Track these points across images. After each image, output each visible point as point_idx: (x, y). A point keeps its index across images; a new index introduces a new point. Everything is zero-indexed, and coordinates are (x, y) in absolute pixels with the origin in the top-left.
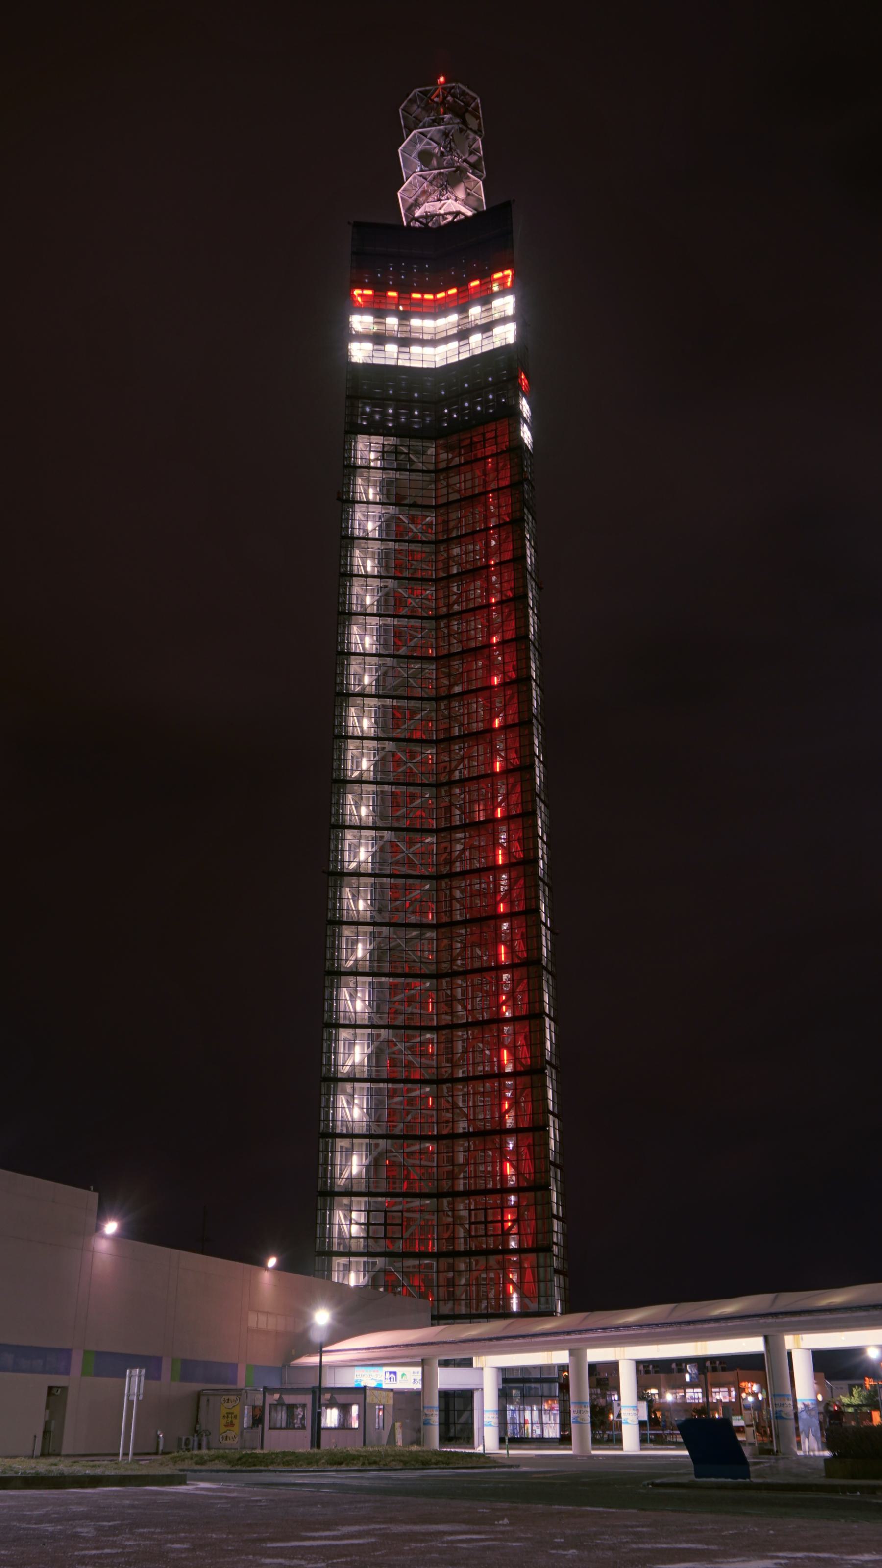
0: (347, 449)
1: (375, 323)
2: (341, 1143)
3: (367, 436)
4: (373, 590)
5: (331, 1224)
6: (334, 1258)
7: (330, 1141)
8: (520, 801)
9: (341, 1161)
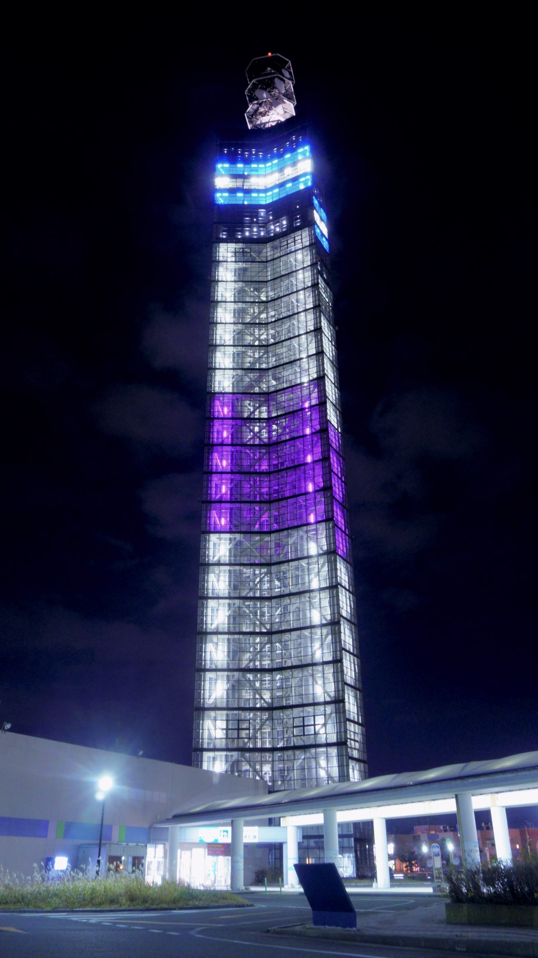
2: (209, 675)
4: (230, 331)
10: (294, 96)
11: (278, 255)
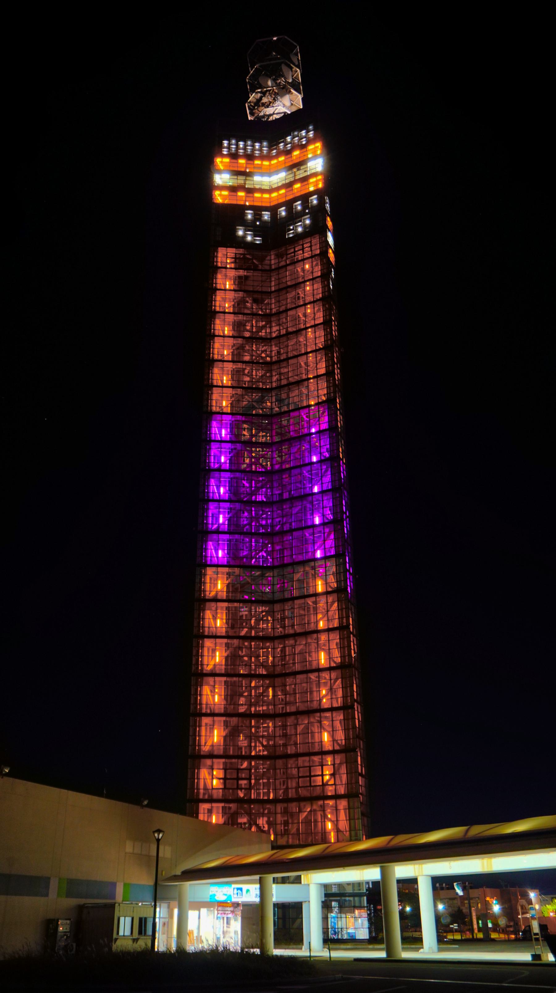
0: (211, 256)
1: (230, 179)
2: (205, 720)
3: (225, 249)
5: (198, 779)
6: (200, 804)
7: (198, 719)
8: (330, 481)
9: (206, 733)
10: (301, 87)
11: (283, 263)
